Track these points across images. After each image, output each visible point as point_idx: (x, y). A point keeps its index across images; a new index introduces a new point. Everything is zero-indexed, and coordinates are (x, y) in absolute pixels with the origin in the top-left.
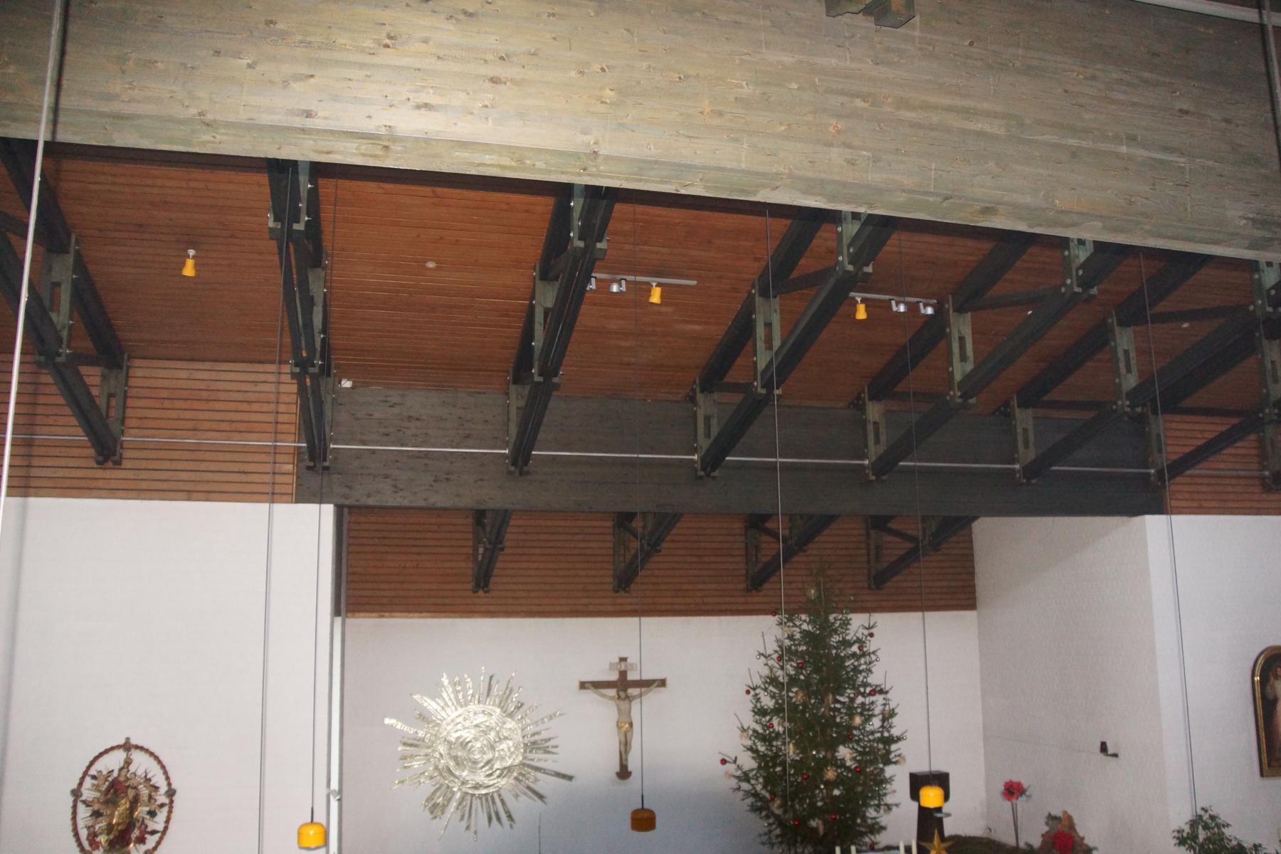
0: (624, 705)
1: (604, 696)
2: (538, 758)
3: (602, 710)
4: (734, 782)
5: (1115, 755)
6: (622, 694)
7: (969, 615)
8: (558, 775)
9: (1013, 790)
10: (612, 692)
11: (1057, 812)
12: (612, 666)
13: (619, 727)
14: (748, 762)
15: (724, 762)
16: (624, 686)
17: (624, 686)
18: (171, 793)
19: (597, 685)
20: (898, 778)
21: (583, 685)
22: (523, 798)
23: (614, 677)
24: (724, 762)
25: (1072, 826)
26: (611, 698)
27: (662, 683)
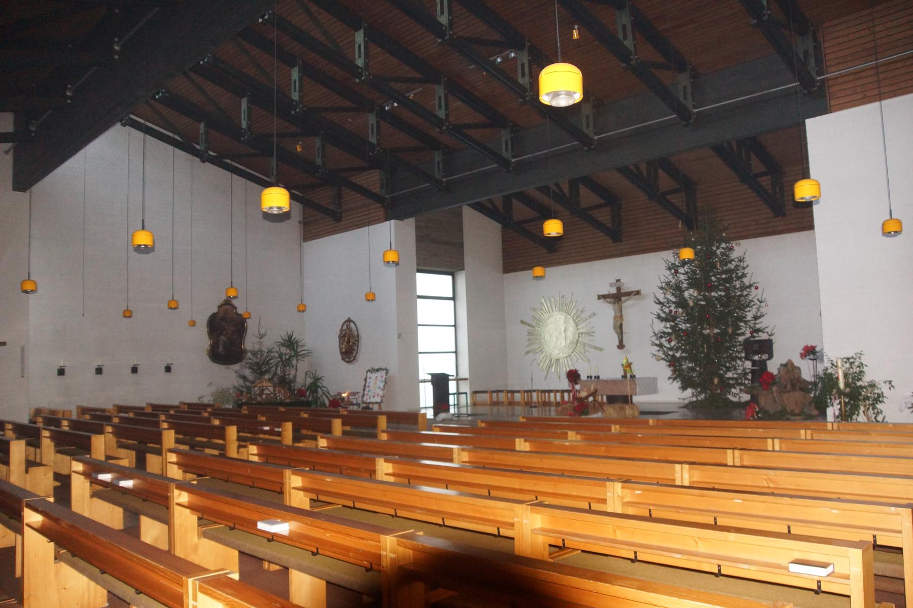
0: (617, 306)
3: (608, 311)
8: (596, 348)
12: (611, 285)
16: (618, 297)
17: (618, 297)
18: (358, 336)
21: (599, 297)
23: (613, 291)
27: (638, 293)
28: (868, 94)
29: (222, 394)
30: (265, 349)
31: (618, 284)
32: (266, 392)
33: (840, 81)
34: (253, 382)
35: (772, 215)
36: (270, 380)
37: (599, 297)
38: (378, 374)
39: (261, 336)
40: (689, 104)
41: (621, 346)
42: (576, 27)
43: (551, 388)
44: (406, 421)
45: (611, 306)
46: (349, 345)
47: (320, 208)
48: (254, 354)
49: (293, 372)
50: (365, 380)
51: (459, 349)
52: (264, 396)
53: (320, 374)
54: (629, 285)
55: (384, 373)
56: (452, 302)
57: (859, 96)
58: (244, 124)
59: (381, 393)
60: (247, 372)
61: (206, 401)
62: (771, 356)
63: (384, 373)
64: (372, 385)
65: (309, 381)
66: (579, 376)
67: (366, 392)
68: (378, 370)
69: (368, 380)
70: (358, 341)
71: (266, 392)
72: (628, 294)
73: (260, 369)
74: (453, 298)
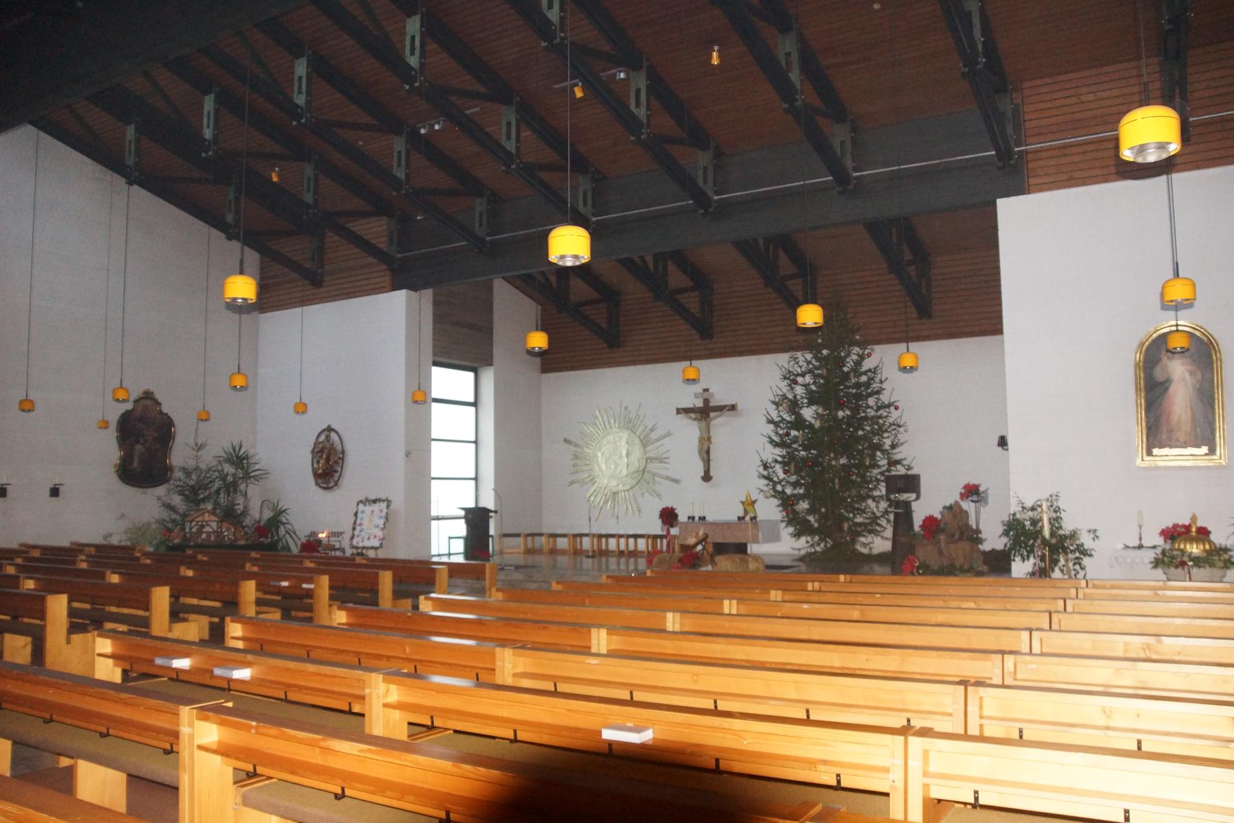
0: (703, 423)
2: (654, 467)
3: (691, 430)
8: (668, 478)
10: (693, 415)
12: (696, 396)
16: (705, 412)
17: (705, 412)
18: (343, 452)
19: (686, 411)
21: (679, 411)
22: (647, 495)
23: (699, 403)
27: (733, 408)
28: (1076, 175)
29: (140, 530)
30: (203, 466)
31: (706, 395)
32: (207, 529)
33: (1044, 154)
34: (185, 516)
35: (915, 315)
36: (213, 512)
37: (679, 411)
38: (376, 507)
39: (199, 447)
40: (849, 163)
41: (707, 477)
42: (716, 48)
43: (622, 532)
44: (417, 576)
45: (696, 423)
46: (328, 465)
47: (295, 267)
48: (188, 473)
49: (240, 500)
50: (356, 514)
51: (480, 476)
52: (204, 536)
53: (283, 505)
54: (719, 399)
55: (384, 505)
56: (473, 409)
57: (1064, 177)
58: (208, 133)
59: (380, 534)
60: (177, 500)
61: (115, 541)
62: (918, 498)
63: (384, 505)
65: (268, 514)
66: (676, 516)
67: (356, 532)
68: (375, 501)
69: (360, 515)
70: (343, 459)
71: (207, 529)
72: (720, 409)
73: (193, 495)
74: (475, 404)
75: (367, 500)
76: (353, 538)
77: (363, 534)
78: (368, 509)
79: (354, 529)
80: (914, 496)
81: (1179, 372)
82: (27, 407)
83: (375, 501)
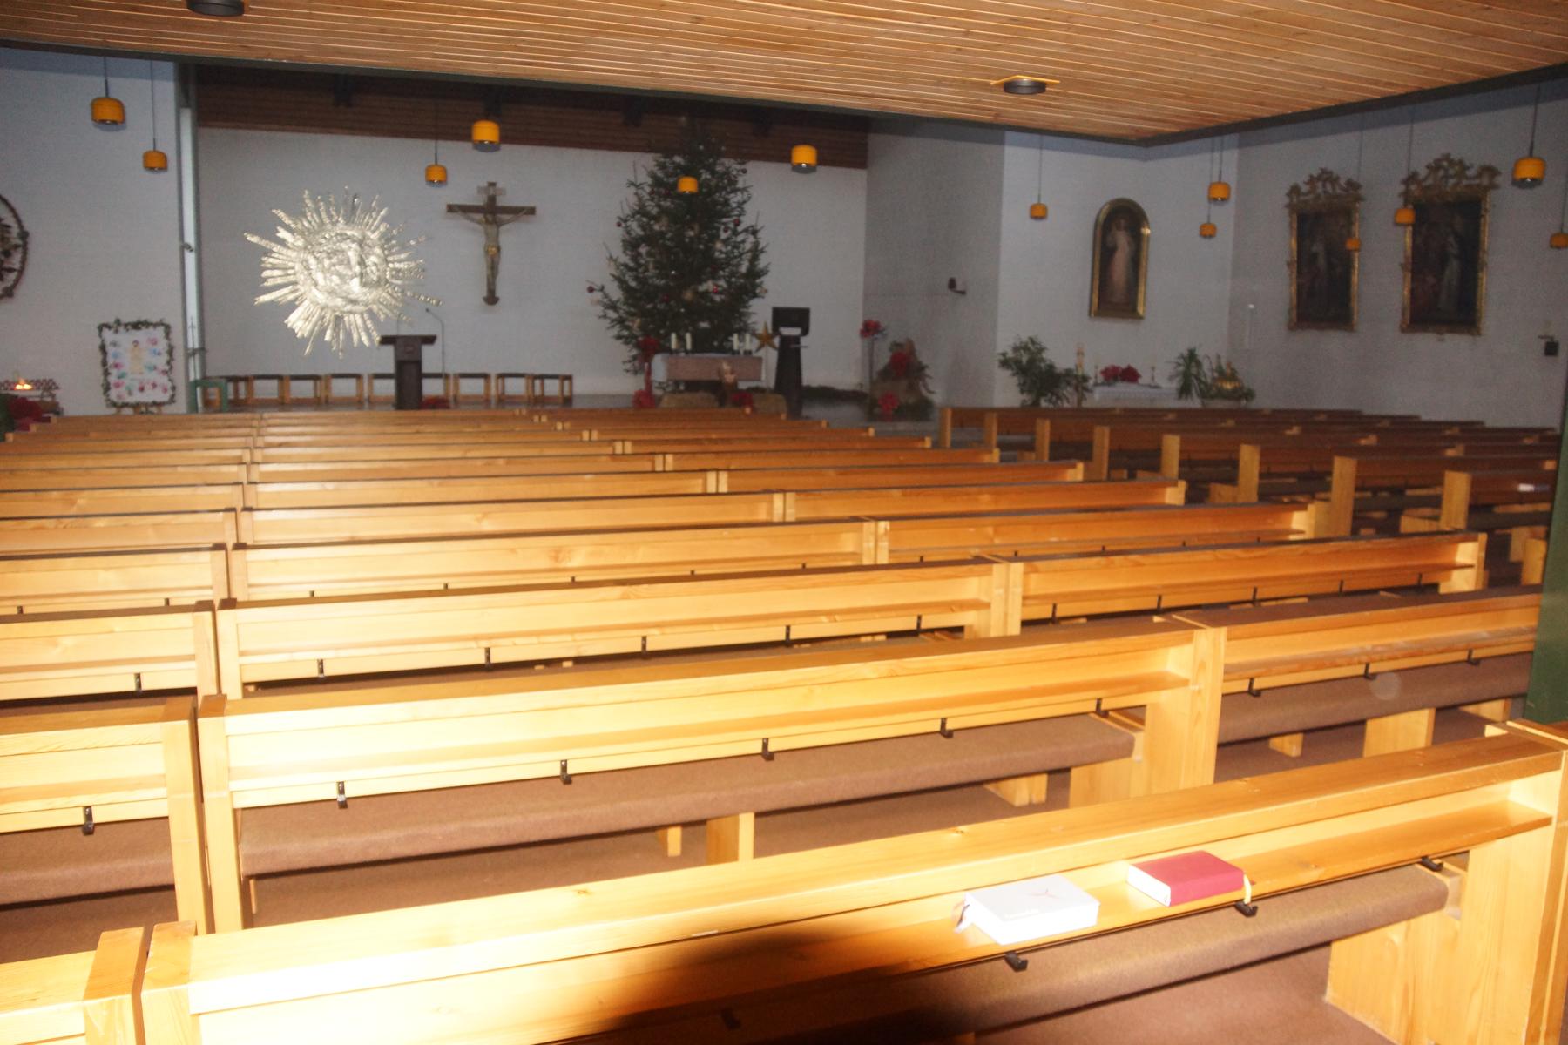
1: (473, 220)
3: (467, 239)
4: (600, 309)
5: (963, 293)
6: (490, 218)
7: (859, 175)
9: (870, 329)
10: (479, 217)
11: (901, 340)
12: (480, 190)
13: (487, 252)
14: (616, 293)
15: (591, 290)
17: (492, 212)
19: (465, 210)
20: (760, 313)
21: (451, 209)
23: (480, 201)
24: (591, 290)
25: (912, 351)
26: (479, 222)
27: (531, 211)
38: (141, 335)
41: (491, 299)
50: (103, 348)
62: (805, 332)
63: (161, 330)
64: (127, 360)
67: (112, 379)
68: (136, 326)
69: (110, 349)
70: (25, 247)
72: (516, 212)
75: (118, 322)
76: (107, 388)
77: (126, 381)
78: (126, 338)
79: (106, 373)
80: (796, 331)
81: (1122, 240)
82: (108, 113)
83: (136, 326)
